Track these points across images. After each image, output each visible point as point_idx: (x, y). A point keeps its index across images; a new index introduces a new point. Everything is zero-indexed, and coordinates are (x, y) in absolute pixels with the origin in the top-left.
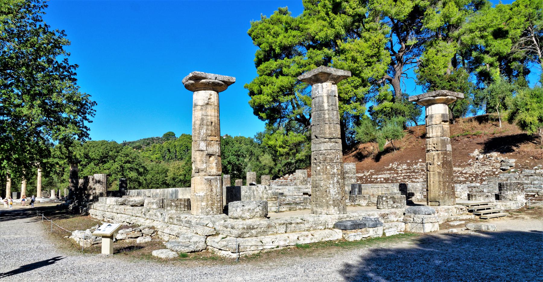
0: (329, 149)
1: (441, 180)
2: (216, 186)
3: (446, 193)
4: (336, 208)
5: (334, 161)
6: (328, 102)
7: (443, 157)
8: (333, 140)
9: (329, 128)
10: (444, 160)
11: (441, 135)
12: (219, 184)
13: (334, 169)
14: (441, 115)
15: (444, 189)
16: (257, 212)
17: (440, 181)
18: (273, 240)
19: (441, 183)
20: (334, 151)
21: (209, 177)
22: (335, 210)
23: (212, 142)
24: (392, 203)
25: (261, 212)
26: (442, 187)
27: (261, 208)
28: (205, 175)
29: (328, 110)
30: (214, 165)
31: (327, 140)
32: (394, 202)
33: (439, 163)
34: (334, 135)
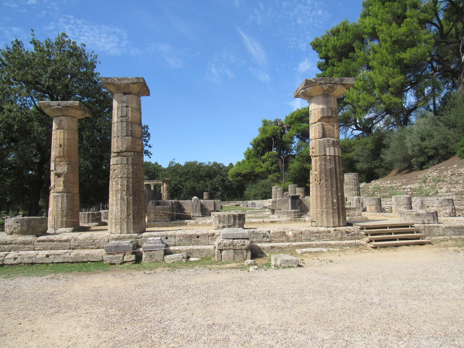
0: (115, 164)
1: (319, 193)
2: (62, 202)
3: (322, 212)
4: (118, 226)
5: (120, 177)
6: (117, 114)
7: (321, 165)
8: (121, 154)
9: (117, 141)
10: (321, 168)
11: (319, 135)
12: (65, 200)
13: (119, 185)
14: (320, 110)
15: (322, 205)
16: (15, 228)
17: (317, 196)
18: (16, 256)
19: (319, 198)
20: (119, 165)
21: (56, 194)
22: (116, 229)
23: (62, 163)
24: (218, 222)
25: (19, 228)
26: (319, 203)
27: (19, 224)
28: (53, 193)
29: (117, 122)
30: (62, 182)
31: (116, 154)
32: (220, 222)
33: (317, 173)
34: (121, 148)
